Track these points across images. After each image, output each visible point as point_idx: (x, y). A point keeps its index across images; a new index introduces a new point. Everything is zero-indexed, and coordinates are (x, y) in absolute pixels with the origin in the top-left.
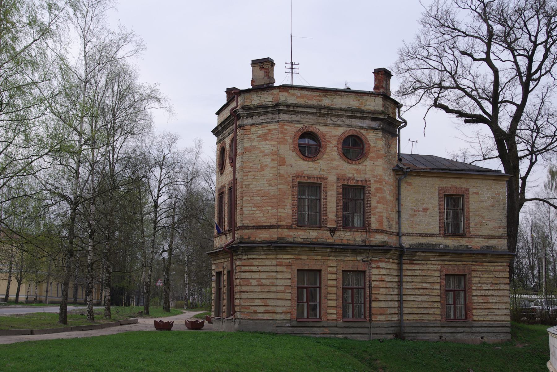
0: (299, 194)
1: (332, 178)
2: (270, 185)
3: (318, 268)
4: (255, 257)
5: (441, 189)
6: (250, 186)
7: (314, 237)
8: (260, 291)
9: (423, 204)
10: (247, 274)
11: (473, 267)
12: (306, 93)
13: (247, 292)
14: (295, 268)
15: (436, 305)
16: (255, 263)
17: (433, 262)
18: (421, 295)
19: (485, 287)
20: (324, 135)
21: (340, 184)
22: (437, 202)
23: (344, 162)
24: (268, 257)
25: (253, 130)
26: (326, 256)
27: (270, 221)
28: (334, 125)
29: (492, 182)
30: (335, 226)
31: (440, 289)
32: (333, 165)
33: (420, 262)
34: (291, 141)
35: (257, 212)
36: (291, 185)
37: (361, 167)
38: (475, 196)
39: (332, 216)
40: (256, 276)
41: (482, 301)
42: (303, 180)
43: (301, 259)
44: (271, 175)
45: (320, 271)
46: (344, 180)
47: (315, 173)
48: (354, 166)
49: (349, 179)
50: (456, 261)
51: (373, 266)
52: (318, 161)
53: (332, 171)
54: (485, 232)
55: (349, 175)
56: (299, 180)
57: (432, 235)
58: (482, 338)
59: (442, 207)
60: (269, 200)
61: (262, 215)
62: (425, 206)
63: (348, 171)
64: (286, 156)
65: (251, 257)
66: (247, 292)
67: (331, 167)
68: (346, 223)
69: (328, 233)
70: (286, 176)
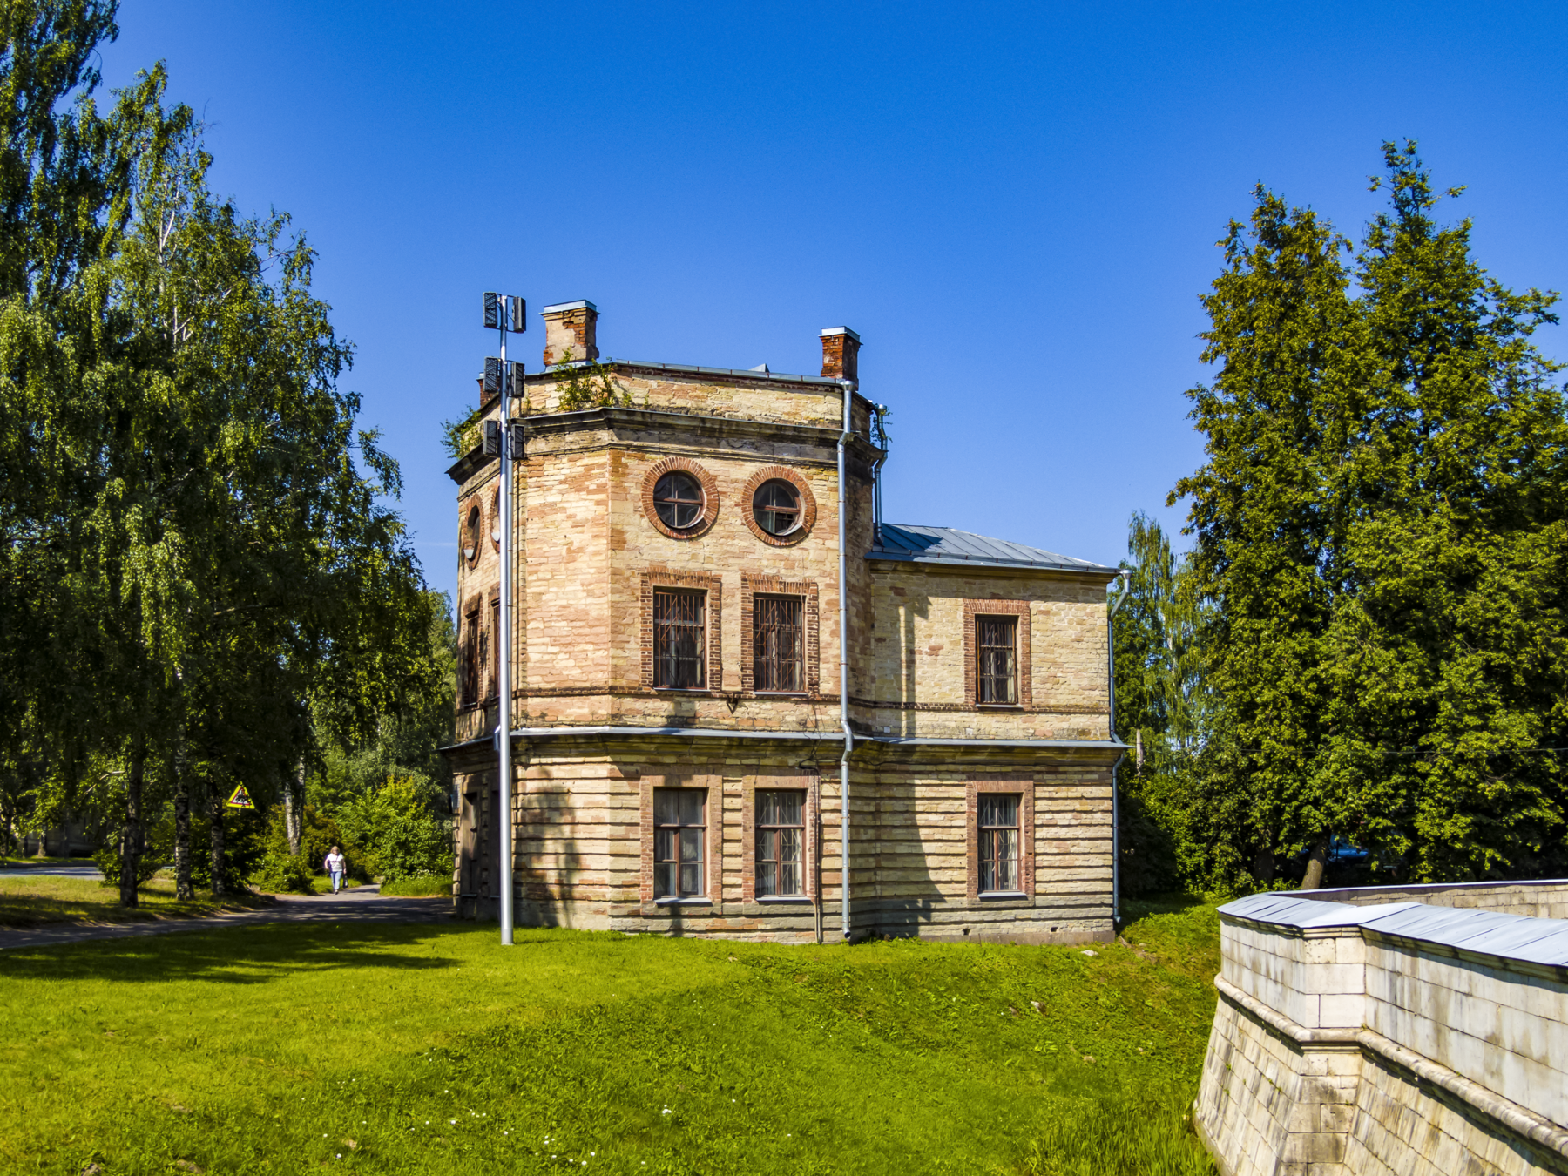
0: (656, 617)
1: (732, 580)
2: (590, 594)
15: (955, 862)
17: (952, 767)
19: (1061, 819)
20: (712, 479)
21: (750, 592)
22: (962, 631)
26: (718, 756)
27: (591, 676)
29: (1078, 586)
30: (739, 688)
33: (922, 768)
34: (639, 492)
35: (562, 656)
36: (639, 593)
37: (795, 552)
38: (1041, 618)
42: (666, 583)
43: (663, 764)
46: (758, 582)
47: (694, 567)
49: (769, 580)
50: (1001, 764)
53: (731, 561)
54: (1062, 698)
55: (767, 571)
57: (951, 708)
58: (1054, 929)
59: (972, 644)
60: (587, 630)
61: (572, 663)
62: (933, 642)
63: (765, 563)
64: (626, 528)
67: (731, 554)
68: (760, 677)
70: (628, 573)
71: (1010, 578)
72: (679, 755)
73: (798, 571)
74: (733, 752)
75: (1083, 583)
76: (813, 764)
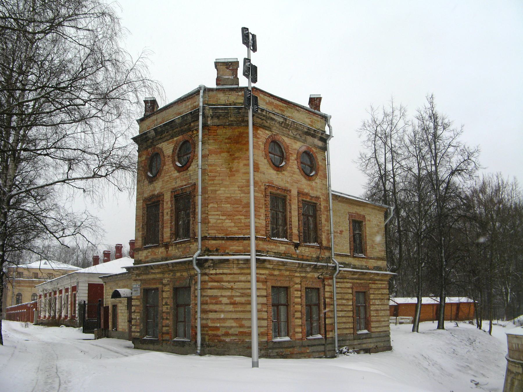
1: (294, 192)
3: (286, 284)
4: (225, 271)
5: (351, 215)
6: (218, 192)
7: (283, 252)
8: (233, 310)
9: (340, 226)
10: (215, 291)
11: (370, 285)
12: (273, 101)
13: (216, 312)
14: (269, 284)
16: (225, 278)
17: (348, 280)
18: (341, 311)
21: (300, 199)
23: (302, 177)
24: (243, 271)
25: (220, 132)
28: (295, 138)
31: (353, 305)
32: (295, 179)
35: (227, 221)
36: (264, 193)
37: (313, 184)
39: (295, 231)
40: (228, 293)
41: (376, 315)
44: (244, 181)
45: (287, 288)
48: (309, 182)
49: (307, 194)
51: (326, 283)
52: (283, 172)
55: (306, 191)
56: (270, 190)
61: (233, 224)
62: (341, 229)
64: (259, 163)
65: (221, 271)
66: (216, 312)
69: (293, 248)
70: (260, 184)
71: (360, 206)
72: (280, 270)
73: (315, 192)
74: (298, 270)
75: (378, 210)
76: (322, 277)
